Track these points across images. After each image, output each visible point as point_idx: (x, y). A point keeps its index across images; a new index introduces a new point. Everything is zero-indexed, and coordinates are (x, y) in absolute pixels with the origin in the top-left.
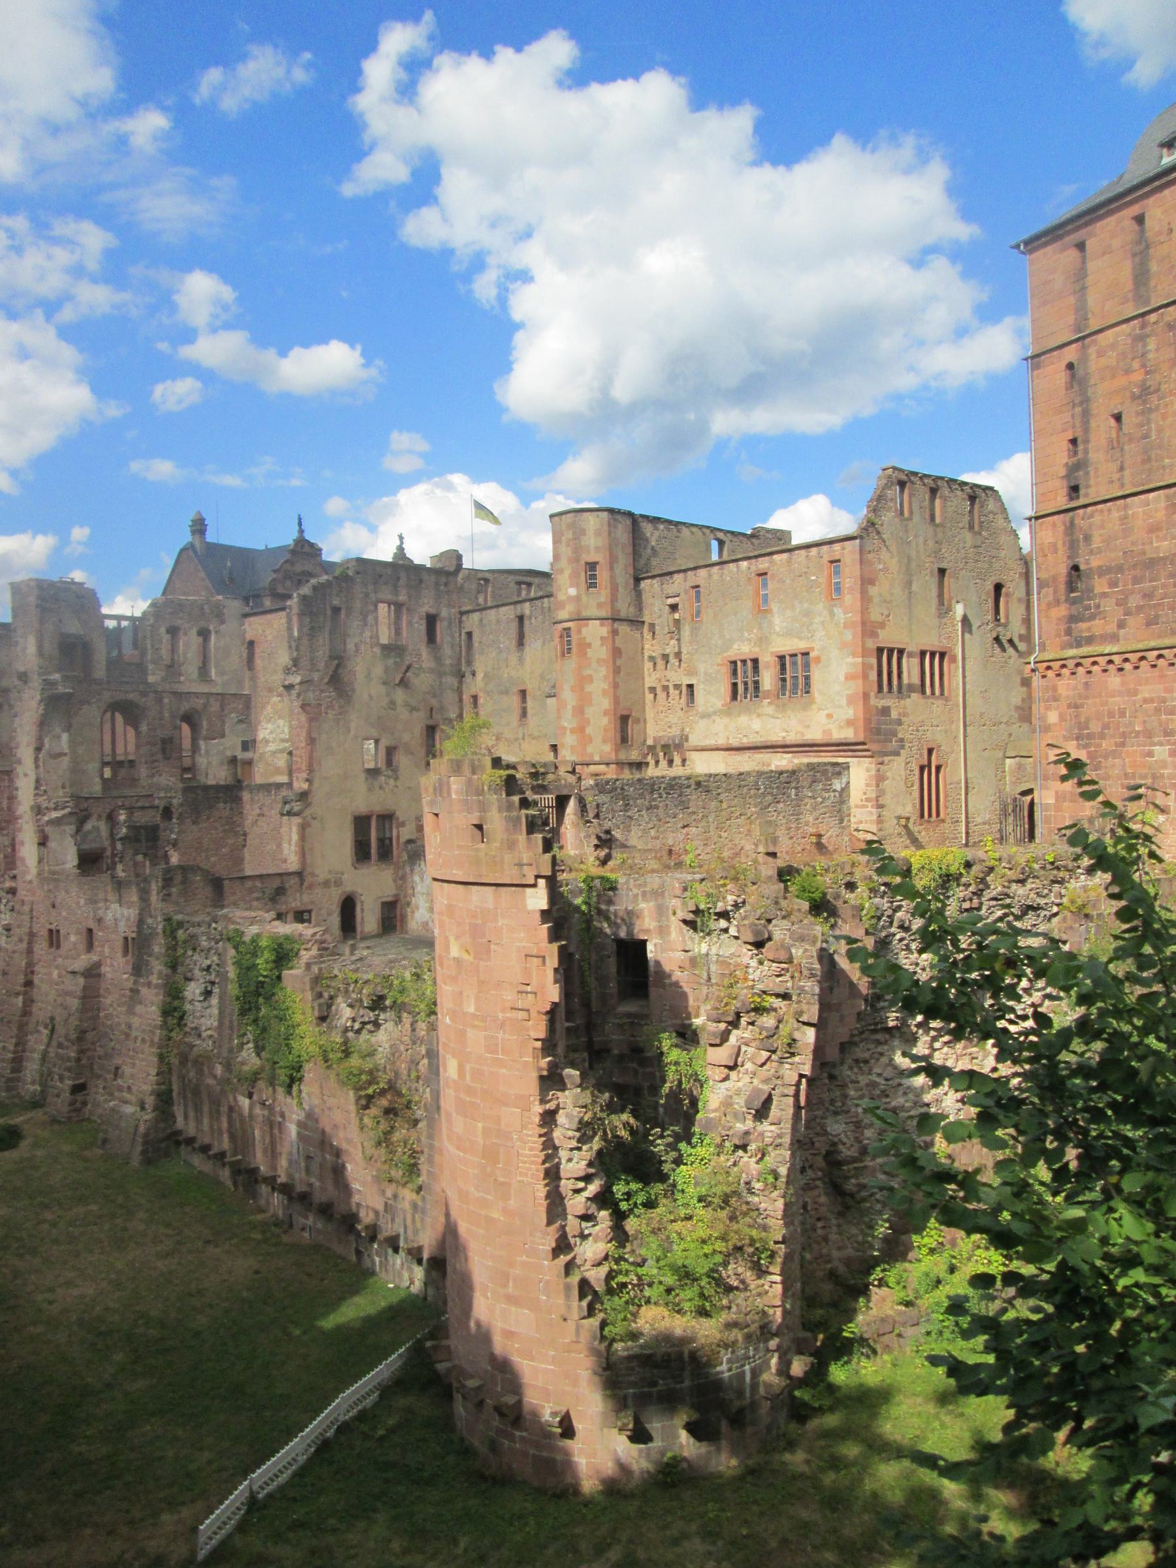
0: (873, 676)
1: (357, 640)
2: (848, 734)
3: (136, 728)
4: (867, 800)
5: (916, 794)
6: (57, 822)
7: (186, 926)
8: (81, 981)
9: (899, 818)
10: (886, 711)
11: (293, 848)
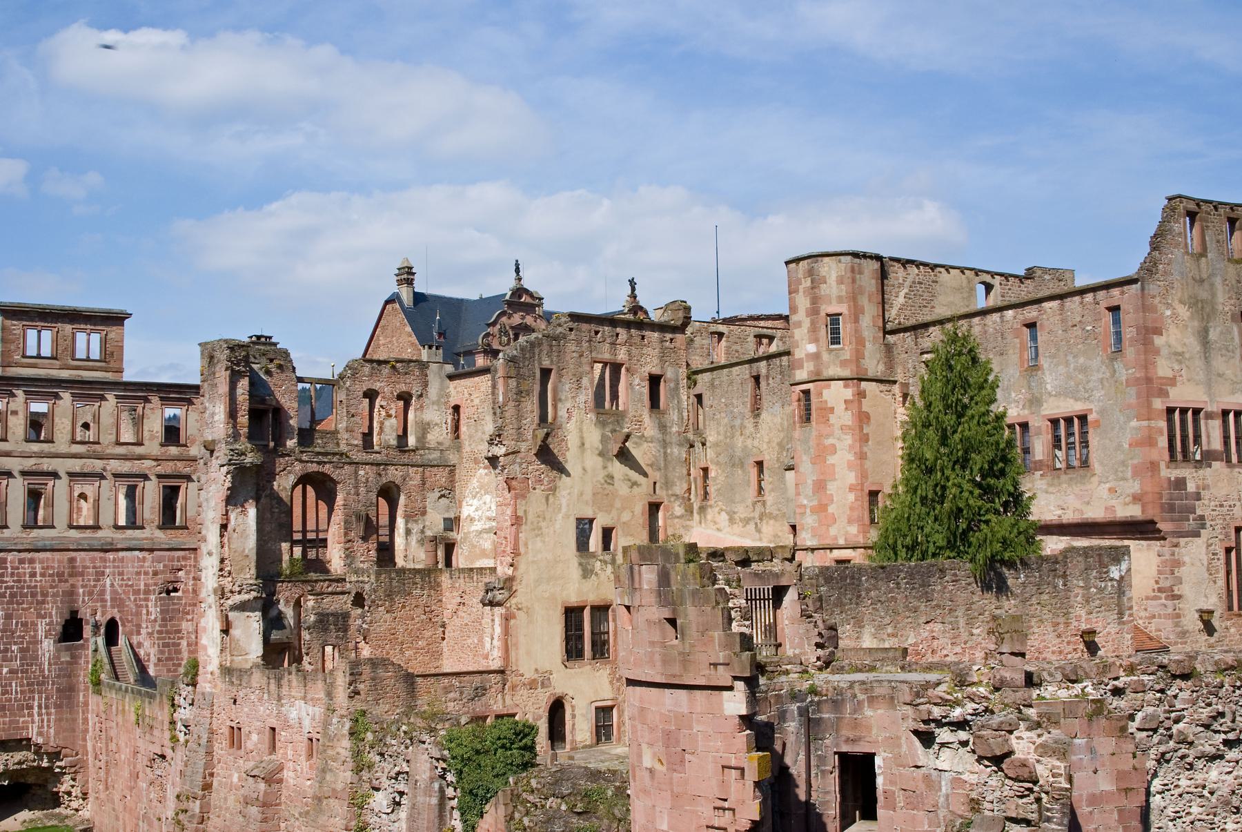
0: (1163, 442)
1: (568, 405)
2: (1134, 512)
4: (1160, 590)
5: (1221, 582)
9: (1201, 611)
10: (1180, 483)
11: (496, 642)
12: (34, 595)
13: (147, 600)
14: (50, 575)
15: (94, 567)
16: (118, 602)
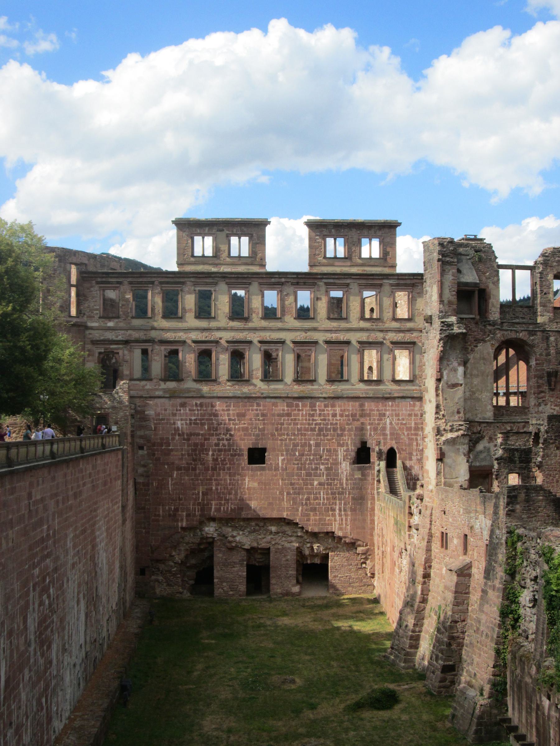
3: (527, 362)
6: (452, 442)
7: (525, 539)
8: (455, 578)
12: (335, 430)
13: (416, 435)
14: (347, 416)
15: (378, 410)
16: (395, 436)
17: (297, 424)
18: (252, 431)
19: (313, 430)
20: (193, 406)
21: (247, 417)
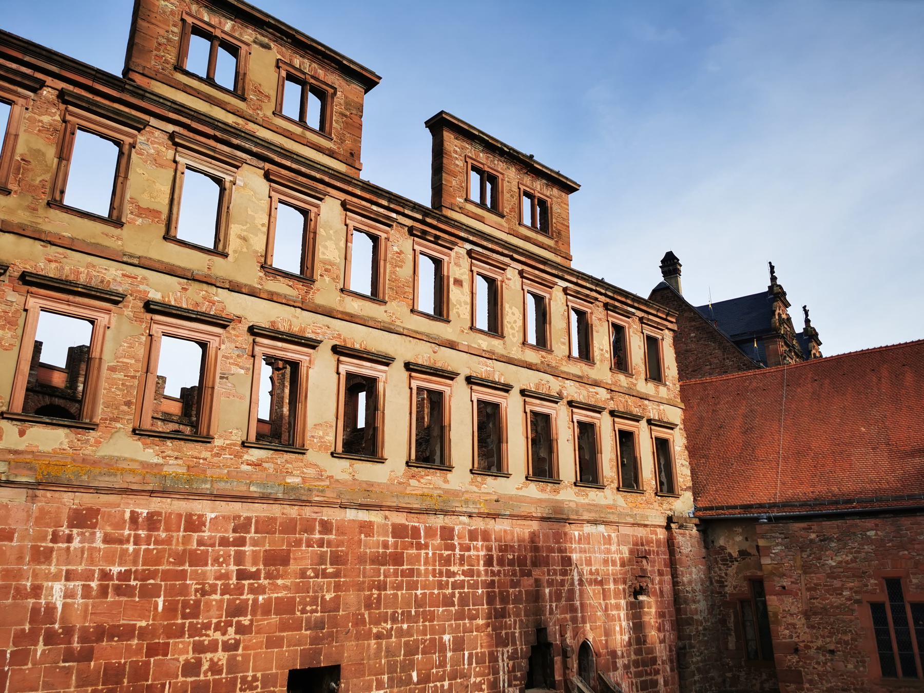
14: (511, 563)
17: (413, 586)
18: (303, 611)
19: (448, 602)
20: (120, 525)
21: (293, 567)
